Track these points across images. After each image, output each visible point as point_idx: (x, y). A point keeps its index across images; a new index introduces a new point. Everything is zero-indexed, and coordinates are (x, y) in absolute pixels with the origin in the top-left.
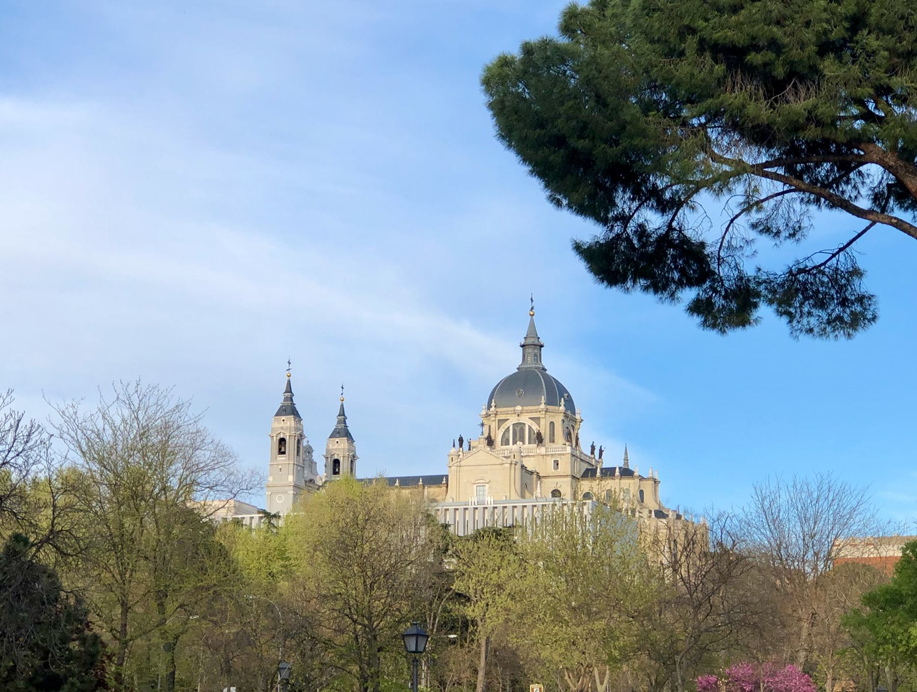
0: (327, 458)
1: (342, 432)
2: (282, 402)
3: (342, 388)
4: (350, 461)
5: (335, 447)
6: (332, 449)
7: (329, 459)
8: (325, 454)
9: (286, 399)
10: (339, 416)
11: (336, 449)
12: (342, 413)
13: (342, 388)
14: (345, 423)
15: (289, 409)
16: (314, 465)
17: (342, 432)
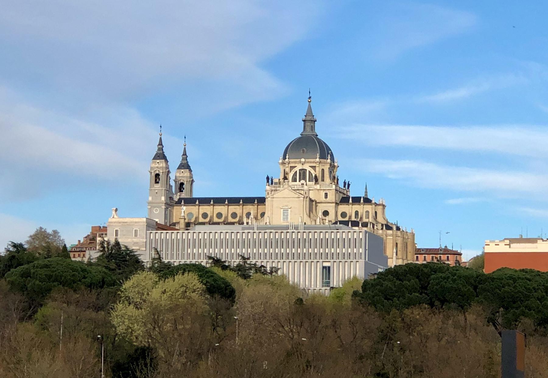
0: (151, 173)
1: (185, 166)
2: (157, 151)
3: (161, 127)
4: (190, 184)
5: (181, 175)
6: (179, 176)
7: (177, 182)
8: (149, 170)
9: (159, 149)
10: (159, 145)
11: (182, 177)
12: (161, 144)
13: (161, 127)
14: (162, 150)
15: (161, 156)
16: (171, 187)
17: (185, 166)
